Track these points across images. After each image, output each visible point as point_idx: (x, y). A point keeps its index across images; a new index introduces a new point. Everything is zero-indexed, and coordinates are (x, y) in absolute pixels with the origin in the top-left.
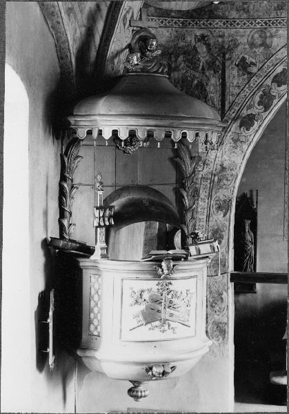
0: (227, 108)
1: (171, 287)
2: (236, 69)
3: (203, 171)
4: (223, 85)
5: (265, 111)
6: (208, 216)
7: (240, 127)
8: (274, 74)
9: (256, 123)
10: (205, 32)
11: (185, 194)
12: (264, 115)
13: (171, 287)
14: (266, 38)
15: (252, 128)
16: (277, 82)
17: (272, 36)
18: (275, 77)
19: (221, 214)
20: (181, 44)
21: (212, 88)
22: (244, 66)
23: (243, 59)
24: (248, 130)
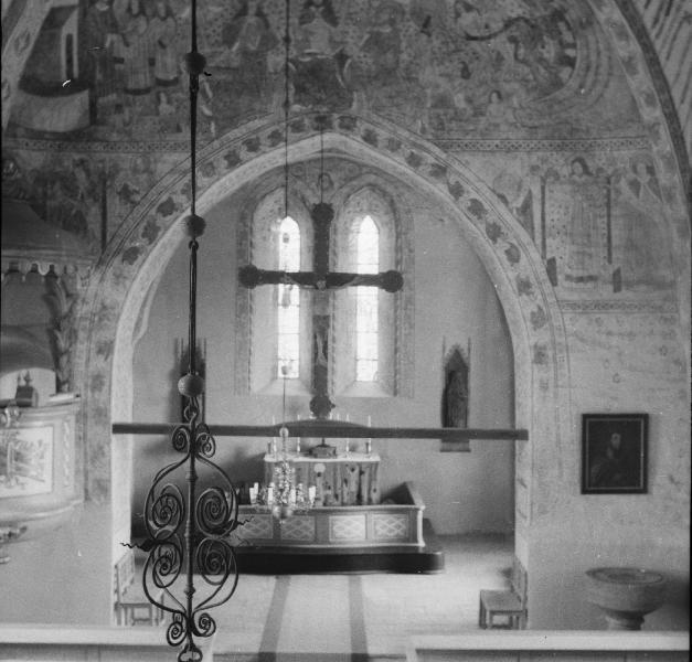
0: (108, 239)
1: (18, 437)
3: (81, 310)
5: (150, 243)
6: (88, 360)
8: (160, 202)
10: (84, 156)
11: (59, 335)
12: (149, 247)
13: (18, 437)
15: (135, 263)
16: (163, 212)
17: (155, 162)
18: (162, 205)
19: (102, 357)
20: (58, 169)
22: (126, 194)
23: (126, 188)
24: (131, 264)
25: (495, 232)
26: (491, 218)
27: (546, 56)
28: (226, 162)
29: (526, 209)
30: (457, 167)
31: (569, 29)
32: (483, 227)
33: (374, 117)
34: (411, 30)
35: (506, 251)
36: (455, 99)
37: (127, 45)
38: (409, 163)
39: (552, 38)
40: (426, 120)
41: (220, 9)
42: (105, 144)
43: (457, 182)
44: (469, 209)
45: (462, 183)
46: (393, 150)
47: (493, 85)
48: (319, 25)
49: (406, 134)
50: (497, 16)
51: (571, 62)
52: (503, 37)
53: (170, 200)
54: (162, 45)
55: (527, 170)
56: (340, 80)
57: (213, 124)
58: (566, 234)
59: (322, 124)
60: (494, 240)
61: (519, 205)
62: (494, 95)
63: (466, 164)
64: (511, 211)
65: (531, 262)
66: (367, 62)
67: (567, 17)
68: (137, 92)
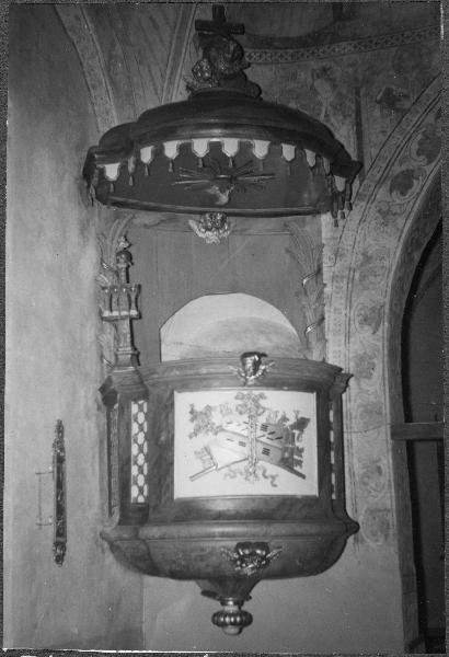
5: (430, 162)
7: (391, 191)
9: (415, 182)
10: (325, 63)
13: (262, 403)
14: (421, 56)
15: (410, 192)
23: (389, 92)
24: (403, 194)
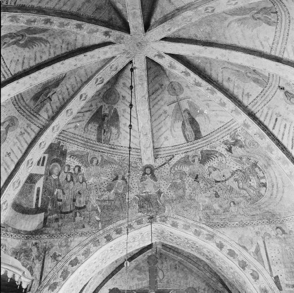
0: (42, 280)
2: (51, 258)
4: (43, 267)
5: (64, 280)
8: (71, 260)
9: (58, 287)
10: (37, 241)
12: (63, 283)
14: (68, 242)
18: (71, 261)
21: (36, 270)
23: (55, 254)
25: (243, 265)
26: (241, 258)
27: (252, 184)
28: (105, 239)
29: (257, 251)
30: (218, 234)
31: (260, 170)
32: (237, 263)
33: (176, 216)
34: (190, 180)
35: (251, 274)
36: (214, 205)
37: (64, 194)
38: (195, 234)
39: (254, 176)
40: (201, 215)
41: (106, 178)
42: (48, 235)
43: (220, 242)
44: (228, 254)
45: (223, 242)
46: (186, 229)
47: (230, 199)
48: (149, 180)
49: (192, 222)
50: (228, 171)
51: (265, 185)
52: (232, 179)
53: (76, 259)
54: (79, 193)
55: (254, 234)
56: (159, 202)
57: (100, 223)
58: (281, 263)
59: (152, 219)
60: (243, 268)
61: (253, 251)
62: (232, 204)
63: (223, 233)
64: (250, 254)
65: (265, 279)
66: (172, 194)
67: (258, 165)
68: (65, 213)
